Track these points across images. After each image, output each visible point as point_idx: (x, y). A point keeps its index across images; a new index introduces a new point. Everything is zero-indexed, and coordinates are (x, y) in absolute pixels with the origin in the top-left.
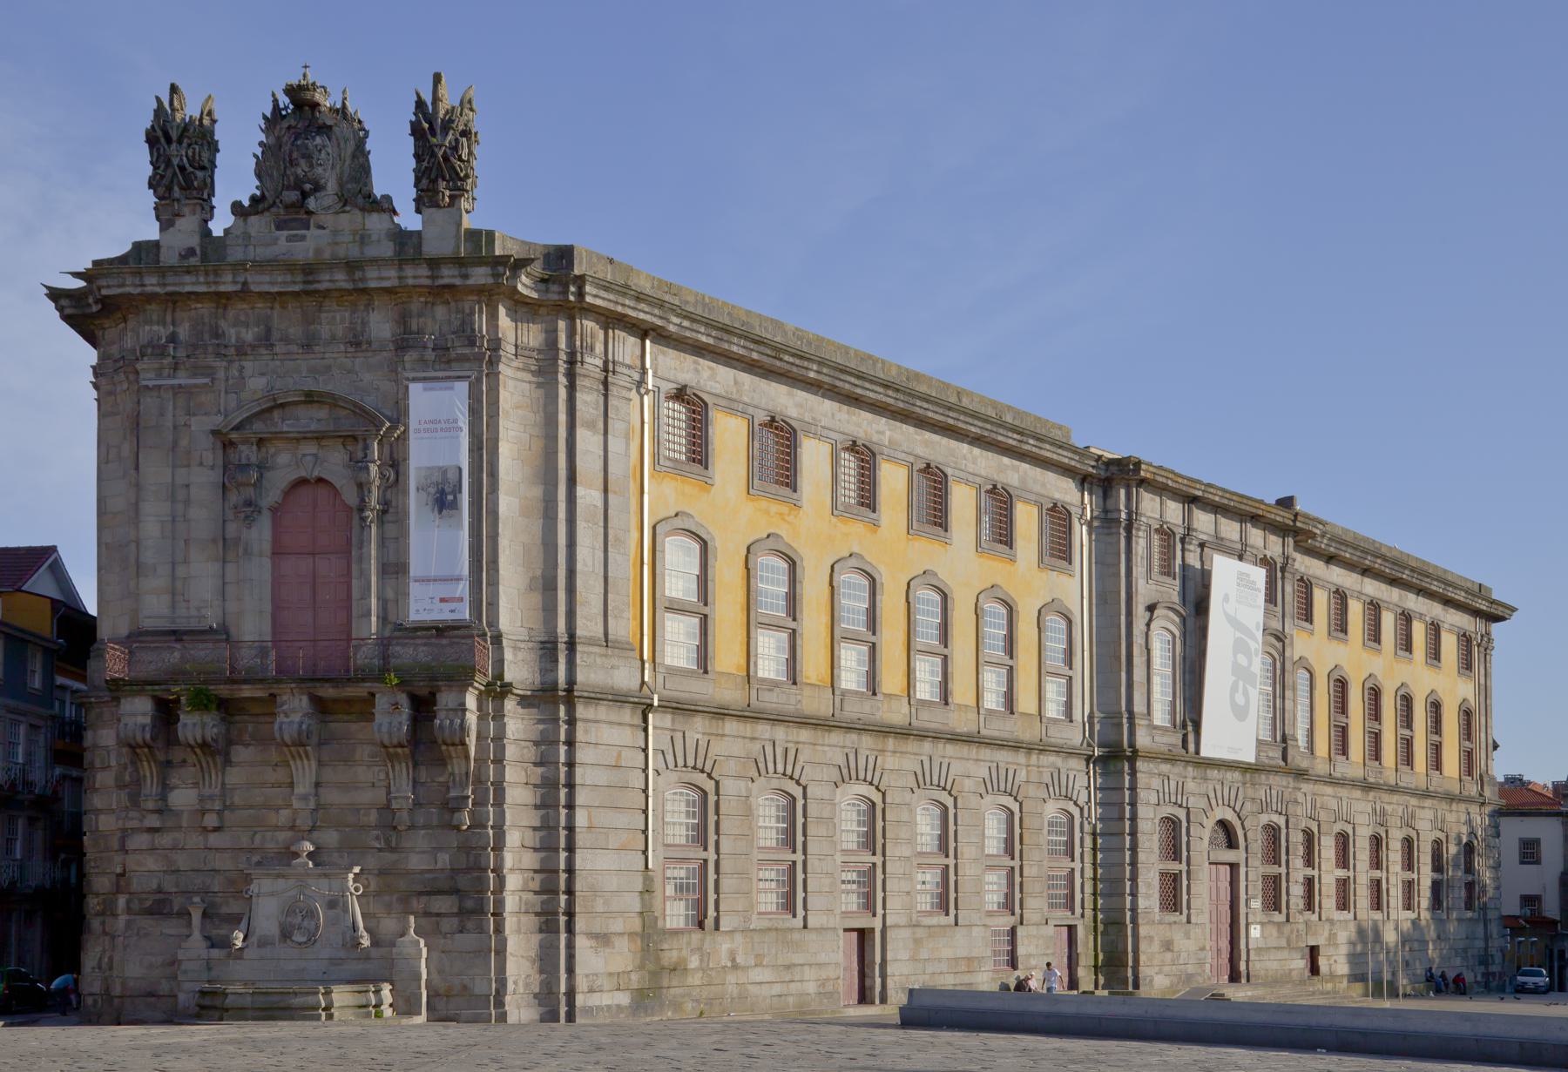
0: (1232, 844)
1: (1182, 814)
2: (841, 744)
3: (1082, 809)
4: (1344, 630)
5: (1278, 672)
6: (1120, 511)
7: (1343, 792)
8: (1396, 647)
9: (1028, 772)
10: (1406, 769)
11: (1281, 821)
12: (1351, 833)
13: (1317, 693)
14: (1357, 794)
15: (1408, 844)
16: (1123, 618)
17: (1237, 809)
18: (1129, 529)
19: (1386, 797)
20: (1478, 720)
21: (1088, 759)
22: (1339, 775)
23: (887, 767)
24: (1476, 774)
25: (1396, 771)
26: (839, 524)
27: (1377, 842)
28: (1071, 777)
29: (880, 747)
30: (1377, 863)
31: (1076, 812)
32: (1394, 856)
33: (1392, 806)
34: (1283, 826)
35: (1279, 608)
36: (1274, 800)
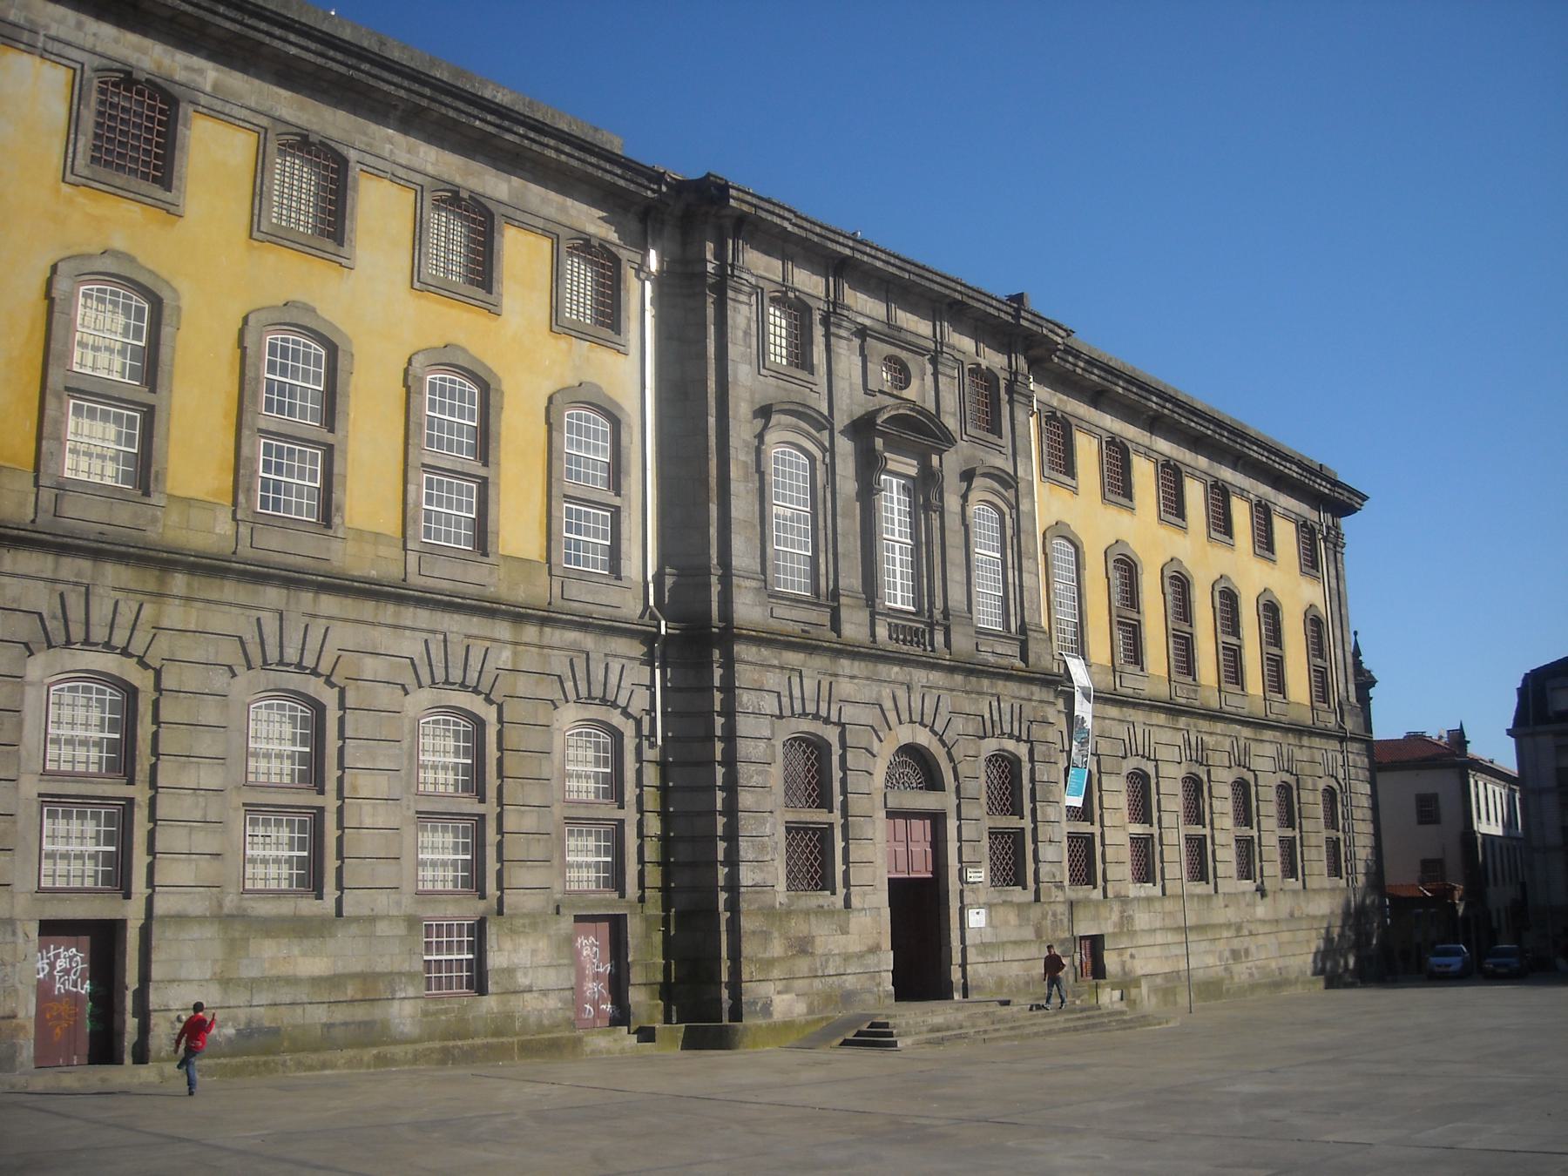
0: (932, 780)
1: (832, 735)
2: (49, 574)
3: (638, 723)
4: (1127, 492)
5: (1009, 532)
6: (705, 261)
7: (1138, 716)
8: (1208, 527)
9: (515, 654)
10: (1235, 689)
11: (1022, 750)
12: (1152, 773)
13: (1088, 575)
14: (1161, 718)
15: (1241, 788)
16: (712, 421)
17: (938, 728)
18: (721, 290)
19: (1204, 725)
20: (1332, 634)
21: (649, 639)
22: (1130, 692)
23: (165, 623)
24: (1334, 700)
25: (1220, 691)
26: (80, 199)
27: (1194, 788)
28: (615, 667)
29: (151, 586)
30: (1195, 814)
31: (628, 729)
32: (1222, 806)
33: (1214, 737)
34: (1025, 758)
35: (1006, 441)
36: (1007, 717)
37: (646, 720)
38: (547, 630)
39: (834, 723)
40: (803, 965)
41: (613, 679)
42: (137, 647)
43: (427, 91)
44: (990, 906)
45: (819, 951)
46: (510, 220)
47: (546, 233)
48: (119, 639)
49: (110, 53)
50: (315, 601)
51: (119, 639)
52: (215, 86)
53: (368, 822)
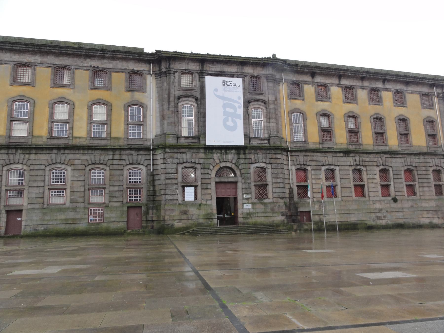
29: (28, 152)
37: (148, 166)
38: (122, 151)
39: (198, 164)
40: (185, 217)
41: (139, 159)
42: (24, 162)
43: (85, 51)
44: (253, 204)
45: (191, 213)
46: (113, 72)
47: (122, 72)
48: (21, 162)
49: (17, 61)
50: (64, 151)
51: (21, 162)
52: (41, 62)
53: (76, 190)
